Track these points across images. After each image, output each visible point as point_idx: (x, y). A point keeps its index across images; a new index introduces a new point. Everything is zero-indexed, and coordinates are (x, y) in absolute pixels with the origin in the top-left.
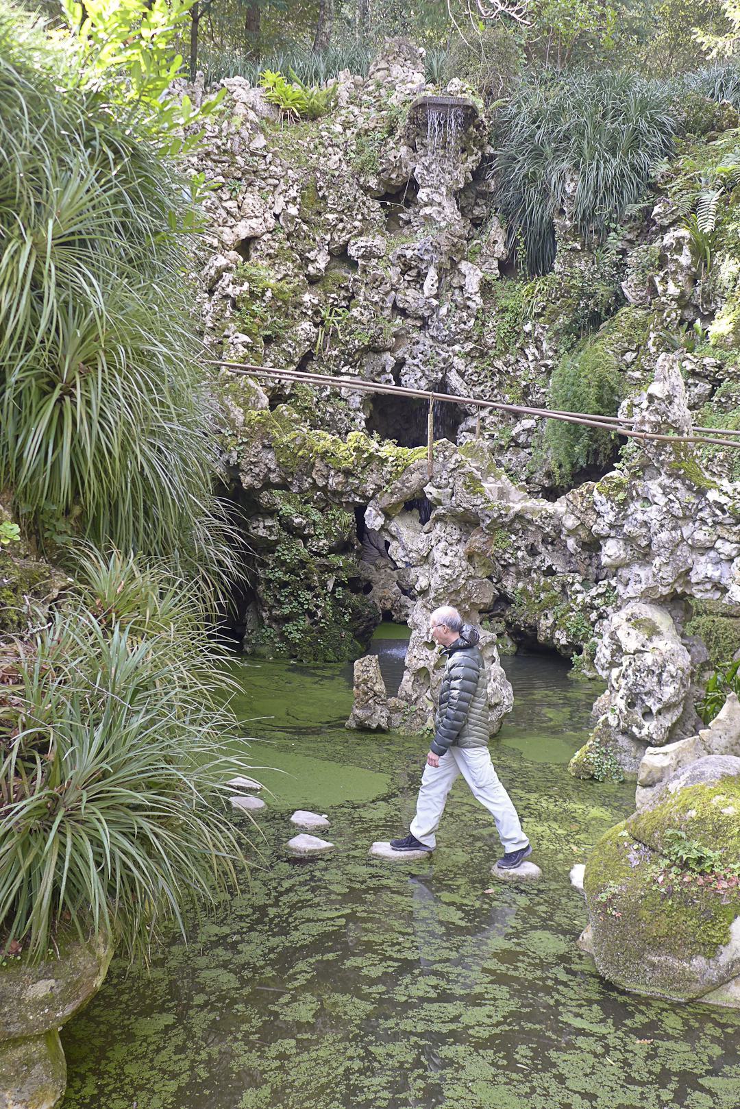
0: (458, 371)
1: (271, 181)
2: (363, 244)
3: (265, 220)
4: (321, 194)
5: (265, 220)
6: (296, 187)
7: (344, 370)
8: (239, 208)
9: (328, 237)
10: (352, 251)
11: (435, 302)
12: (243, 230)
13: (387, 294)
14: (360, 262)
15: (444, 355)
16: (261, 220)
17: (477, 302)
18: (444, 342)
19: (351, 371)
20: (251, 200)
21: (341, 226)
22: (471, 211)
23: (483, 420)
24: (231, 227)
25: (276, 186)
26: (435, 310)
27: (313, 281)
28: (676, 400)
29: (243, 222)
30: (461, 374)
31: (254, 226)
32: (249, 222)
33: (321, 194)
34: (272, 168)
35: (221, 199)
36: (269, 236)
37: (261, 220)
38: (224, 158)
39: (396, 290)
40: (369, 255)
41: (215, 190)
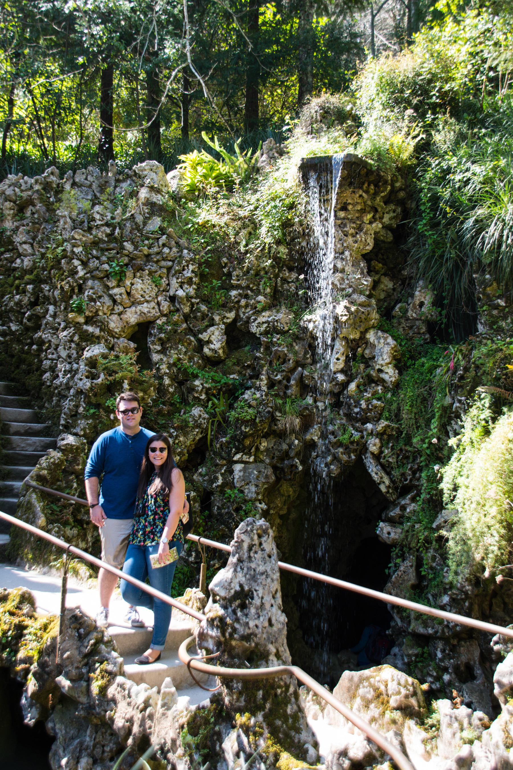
0: (372, 454)
1: (163, 263)
2: (264, 320)
3: (158, 304)
4: (225, 270)
5: (158, 304)
6: (191, 267)
7: (236, 458)
8: (129, 294)
9: (232, 315)
10: (254, 328)
11: (341, 377)
12: (132, 317)
13: (293, 370)
15: (357, 436)
16: (153, 304)
17: (390, 374)
18: (357, 420)
19: (245, 458)
20: (141, 286)
21: (243, 302)
22: (400, 271)
23: (403, 508)
24: (120, 314)
25: (169, 269)
26: (345, 385)
27: (213, 362)
28: (257, 601)
29: (133, 309)
30: (377, 457)
31: (146, 310)
32: (139, 308)
33: (225, 270)
34: (166, 250)
35: (108, 288)
36: (164, 319)
37: (153, 304)
38: (112, 246)
39: (303, 366)
40: (272, 330)
41: (101, 279)
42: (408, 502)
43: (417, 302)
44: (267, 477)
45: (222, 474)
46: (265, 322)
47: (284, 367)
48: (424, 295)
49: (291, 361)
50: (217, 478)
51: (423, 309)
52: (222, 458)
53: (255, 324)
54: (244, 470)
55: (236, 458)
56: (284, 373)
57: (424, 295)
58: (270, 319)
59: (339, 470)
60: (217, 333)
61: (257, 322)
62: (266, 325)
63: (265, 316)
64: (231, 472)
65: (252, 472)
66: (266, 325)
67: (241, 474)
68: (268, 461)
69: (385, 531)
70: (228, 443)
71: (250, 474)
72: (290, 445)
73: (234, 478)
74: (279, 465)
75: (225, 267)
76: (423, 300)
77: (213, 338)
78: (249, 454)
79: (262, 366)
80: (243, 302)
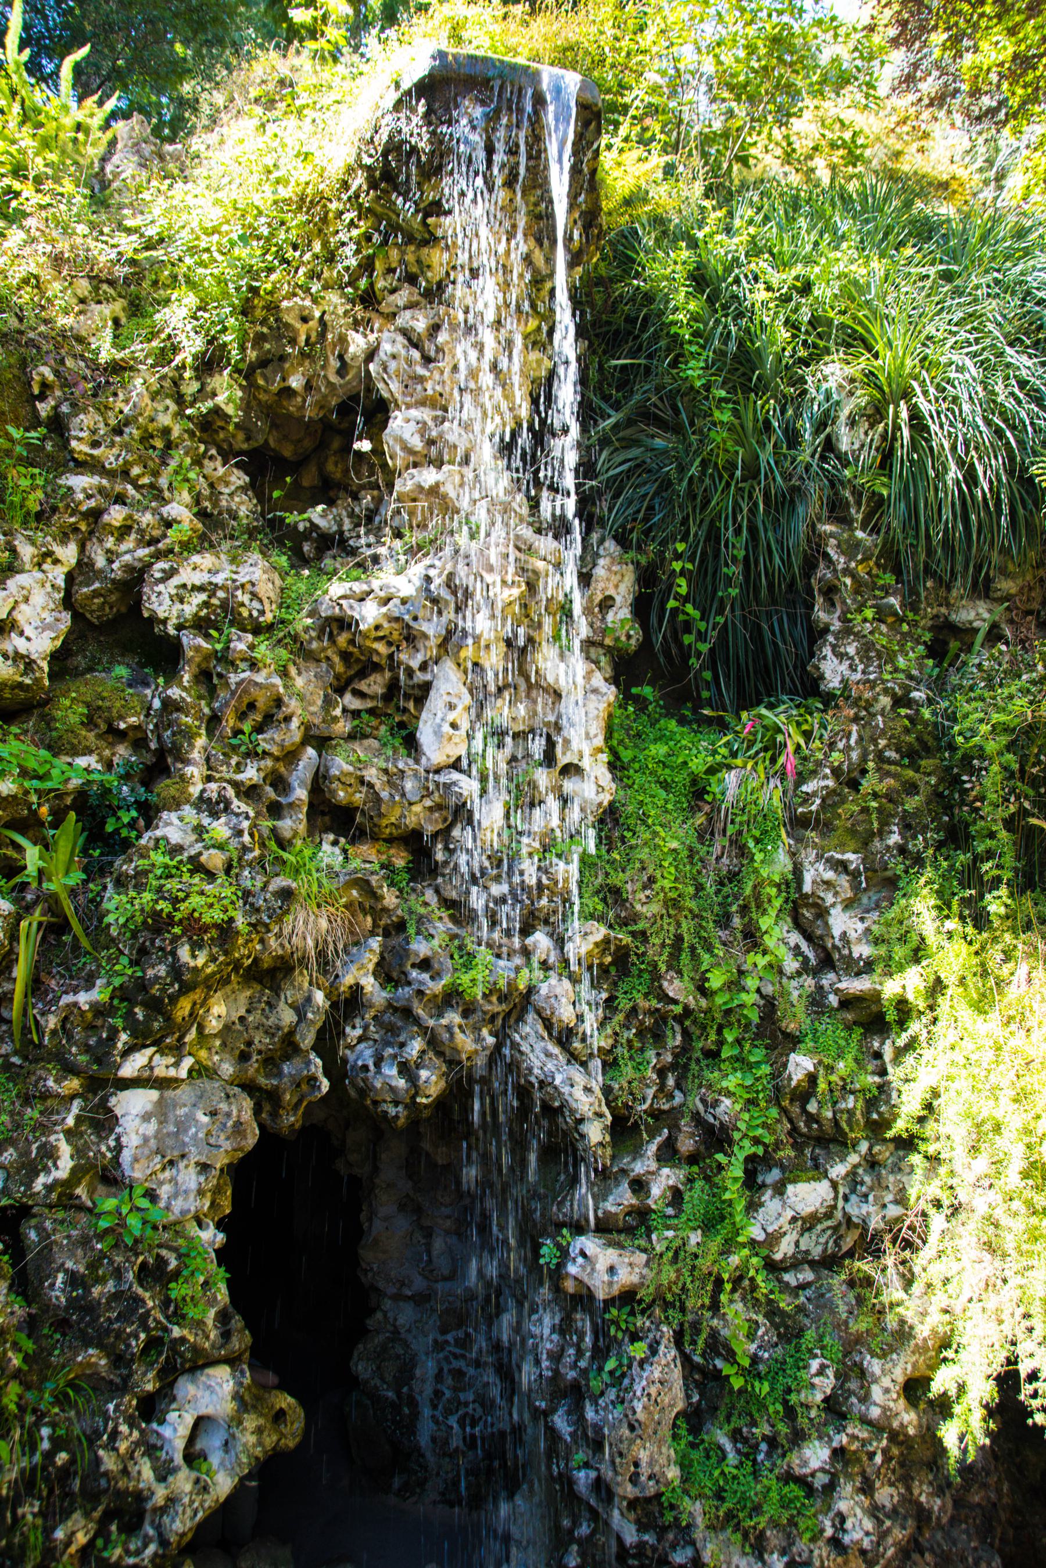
2: (198, 578)
4: (44, 409)
7: (129, 1069)
14: (190, 640)
19: (163, 1066)
23: (639, 1186)
33: (44, 409)
40: (220, 615)
42: (653, 1166)
43: (599, 597)
44: (239, 1128)
45: (70, 1134)
46: (201, 589)
47: (265, 742)
48: (615, 579)
49: (295, 723)
50: (49, 1153)
51: (610, 617)
52: (69, 1069)
53: (170, 587)
54: (161, 1111)
55: (129, 1069)
56: (269, 763)
57: (615, 579)
58: (219, 579)
59: (442, 1084)
60: (39, 598)
61: (175, 581)
62: (203, 597)
63: (200, 568)
64: (103, 1121)
65: (191, 1118)
66: (203, 597)
67: (151, 1128)
68: (227, 1069)
69: (601, 1266)
70: (100, 1010)
71: (182, 1126)
72: (300, 1011)
73: (119, 1148)
74: (262, 1081)
75: (42, 397)
76: (611, 592)
77: (24, 615)
78: (178, 1051)
79: (190, 736)
80: (116, 515)
